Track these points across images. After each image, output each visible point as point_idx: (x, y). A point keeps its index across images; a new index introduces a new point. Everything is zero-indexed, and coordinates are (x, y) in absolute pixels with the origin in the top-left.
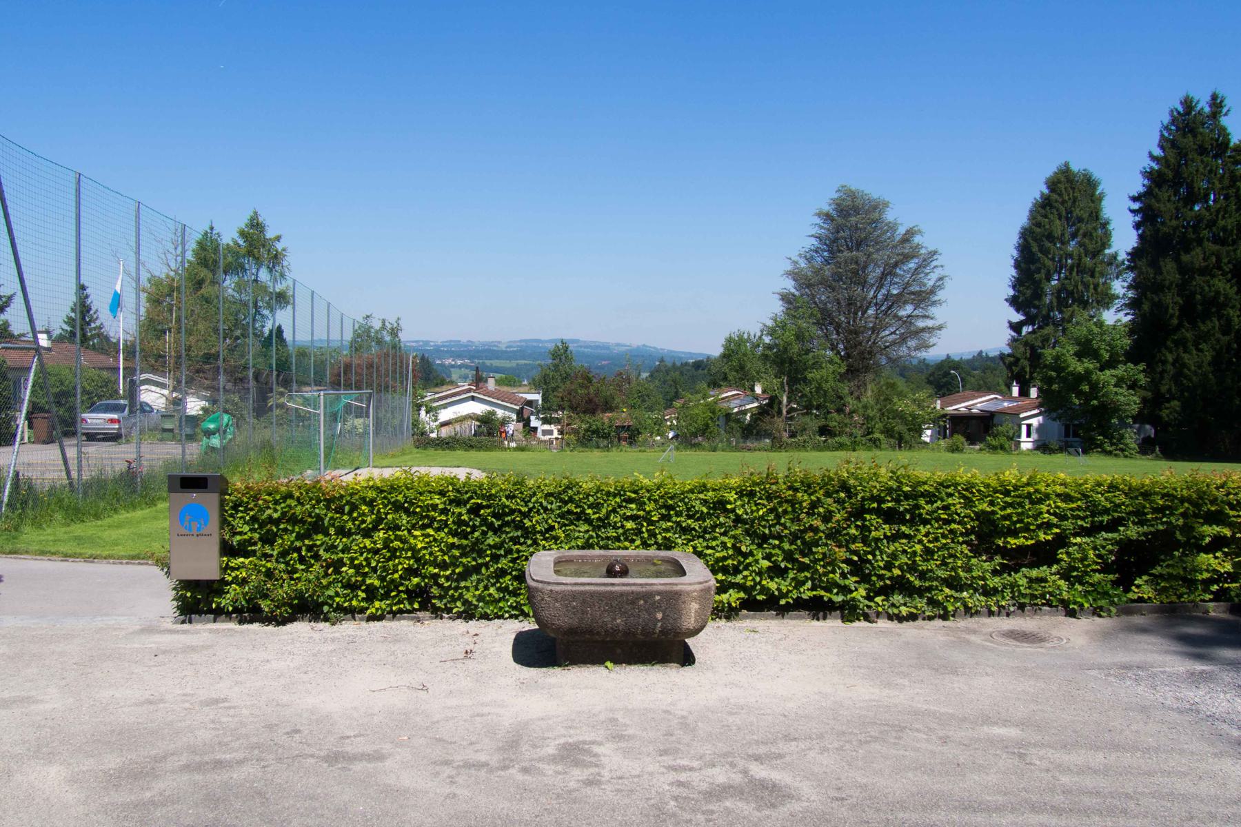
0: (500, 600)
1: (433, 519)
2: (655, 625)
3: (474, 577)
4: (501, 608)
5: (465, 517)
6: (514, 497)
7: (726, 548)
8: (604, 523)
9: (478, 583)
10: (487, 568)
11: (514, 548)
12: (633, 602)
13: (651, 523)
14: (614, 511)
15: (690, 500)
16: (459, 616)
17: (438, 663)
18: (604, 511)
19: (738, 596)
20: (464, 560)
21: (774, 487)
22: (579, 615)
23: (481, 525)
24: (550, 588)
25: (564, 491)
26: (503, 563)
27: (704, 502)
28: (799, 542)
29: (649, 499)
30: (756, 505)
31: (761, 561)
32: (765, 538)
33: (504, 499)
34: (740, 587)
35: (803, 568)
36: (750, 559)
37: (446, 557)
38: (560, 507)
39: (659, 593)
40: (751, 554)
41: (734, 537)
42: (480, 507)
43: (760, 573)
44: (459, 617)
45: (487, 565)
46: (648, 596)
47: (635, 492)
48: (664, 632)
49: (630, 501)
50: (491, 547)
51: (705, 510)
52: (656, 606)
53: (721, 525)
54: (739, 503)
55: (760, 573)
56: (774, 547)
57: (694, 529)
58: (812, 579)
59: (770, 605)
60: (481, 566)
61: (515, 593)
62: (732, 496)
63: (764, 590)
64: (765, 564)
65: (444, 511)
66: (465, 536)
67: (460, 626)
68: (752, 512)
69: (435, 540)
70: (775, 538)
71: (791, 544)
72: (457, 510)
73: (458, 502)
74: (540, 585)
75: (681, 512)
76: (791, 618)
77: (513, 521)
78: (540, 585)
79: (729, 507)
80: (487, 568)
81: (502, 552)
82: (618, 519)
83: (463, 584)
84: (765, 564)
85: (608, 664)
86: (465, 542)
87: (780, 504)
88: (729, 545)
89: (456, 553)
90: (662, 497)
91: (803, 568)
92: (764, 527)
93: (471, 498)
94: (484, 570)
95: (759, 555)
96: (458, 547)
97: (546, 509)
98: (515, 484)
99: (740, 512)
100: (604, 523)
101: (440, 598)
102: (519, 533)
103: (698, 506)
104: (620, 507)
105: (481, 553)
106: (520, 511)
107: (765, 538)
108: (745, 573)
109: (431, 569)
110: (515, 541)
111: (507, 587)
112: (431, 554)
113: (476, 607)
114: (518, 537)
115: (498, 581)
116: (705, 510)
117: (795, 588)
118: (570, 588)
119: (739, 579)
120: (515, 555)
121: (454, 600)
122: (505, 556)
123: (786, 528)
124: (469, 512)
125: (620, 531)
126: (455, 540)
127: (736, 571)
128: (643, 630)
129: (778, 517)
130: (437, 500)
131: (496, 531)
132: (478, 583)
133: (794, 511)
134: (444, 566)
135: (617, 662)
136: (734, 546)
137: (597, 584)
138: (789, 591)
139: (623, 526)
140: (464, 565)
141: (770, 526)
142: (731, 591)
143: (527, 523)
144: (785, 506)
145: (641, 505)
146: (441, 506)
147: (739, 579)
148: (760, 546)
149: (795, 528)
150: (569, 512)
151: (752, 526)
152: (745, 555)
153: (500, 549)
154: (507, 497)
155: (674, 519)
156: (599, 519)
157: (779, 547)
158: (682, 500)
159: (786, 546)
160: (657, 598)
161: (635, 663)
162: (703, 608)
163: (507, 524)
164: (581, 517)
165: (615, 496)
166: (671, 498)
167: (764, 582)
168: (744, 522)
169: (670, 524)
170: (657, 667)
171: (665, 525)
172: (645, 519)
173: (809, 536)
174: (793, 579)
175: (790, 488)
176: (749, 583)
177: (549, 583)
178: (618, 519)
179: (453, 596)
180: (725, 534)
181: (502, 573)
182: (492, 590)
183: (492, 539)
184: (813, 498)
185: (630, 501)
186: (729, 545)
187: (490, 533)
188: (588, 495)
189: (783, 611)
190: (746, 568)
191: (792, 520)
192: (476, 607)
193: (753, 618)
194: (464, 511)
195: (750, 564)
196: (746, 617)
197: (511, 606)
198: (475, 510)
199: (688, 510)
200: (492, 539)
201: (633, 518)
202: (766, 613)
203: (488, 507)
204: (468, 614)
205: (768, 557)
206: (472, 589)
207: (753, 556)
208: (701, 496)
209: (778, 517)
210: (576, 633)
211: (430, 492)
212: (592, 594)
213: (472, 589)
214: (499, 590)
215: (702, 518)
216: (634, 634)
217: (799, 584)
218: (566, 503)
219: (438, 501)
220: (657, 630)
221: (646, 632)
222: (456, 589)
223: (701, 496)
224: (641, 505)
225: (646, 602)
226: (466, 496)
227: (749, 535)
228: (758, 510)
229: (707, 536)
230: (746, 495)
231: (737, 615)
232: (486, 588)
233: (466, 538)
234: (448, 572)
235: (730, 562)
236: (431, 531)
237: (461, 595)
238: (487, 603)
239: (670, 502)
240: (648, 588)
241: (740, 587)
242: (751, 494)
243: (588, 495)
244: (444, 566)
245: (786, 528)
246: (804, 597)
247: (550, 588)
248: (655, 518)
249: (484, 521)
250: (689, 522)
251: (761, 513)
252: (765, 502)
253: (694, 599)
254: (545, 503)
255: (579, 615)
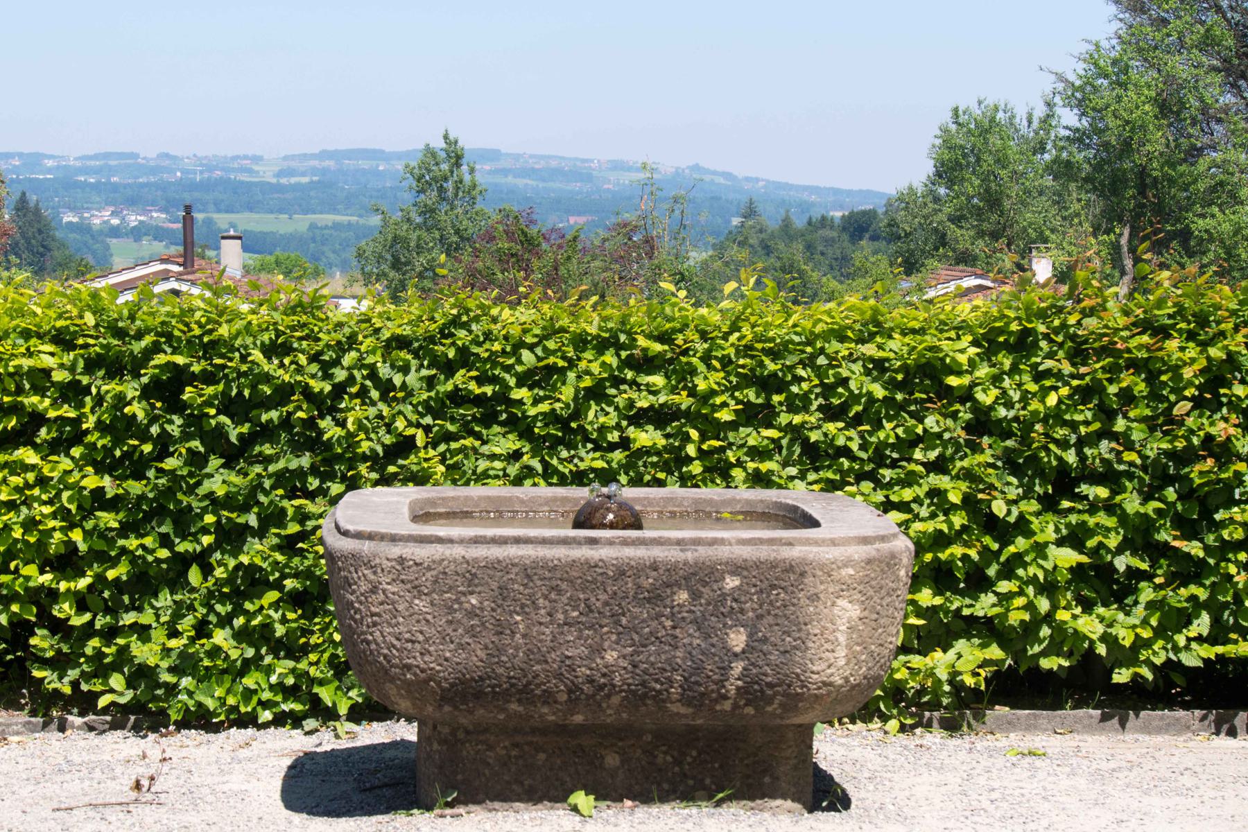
0: (247, 666)
1: (38, 419)
2: (725, 669)
3: (165, 599)
4: (248, 694)
5: (138, 410)
6: (286, 349)
7: (948, 509)
8: (567, 431)
9: (177, 616)
10: (207, 570)
11: (289, 506)
12: (655, 597)
13: (712, 428)
14: (596, 393)
15: (833, 360)
16: (120, 717)
17: (48, 813)
18: (567, 393)
19: (981, 655)
20: (132, 543)
21: (1091, 323)
22: (489, 638)
23: (186, 437)
24: (396, 551)
25: (445, 333)
26: (255, 552)
27: (878, 367)
28: (1171, 493)
29: (706, 358)
30: (1038, 376)
31: (1052, 551)
32: (1064, 483)
33: (257, 355)
34: (989, 629)
35: (1188, 571)
36: (1021, 544)
37: (77, 536)
38: (430, 382)
39: (737, 568)
40: (1023, 526)
41: (968, 475)
42: (180, 377)
43: (1049, 588)
44: (115, 726)
45: (203, 560)
46: (700, 577)
47: (663, 338)
48: (753, 692)
49: (647, 364)
50: (214, 502)
51: (879, 392)
52: (725, 610)
53: (927, 439)
54: (983, 371)
55: (1049, 588)
56: (1093, 508)
57: (846, 452)
58: (1213, 607)
59: (1089, 687)
60: (182, 562)
61: (291, 648)
62: (963, 351)
63: (1063, 640)
64: (1067, 557)
65: (72, 392)
66: (136, 467)
67: (124, 749)
68: (1025, 398)
69: (42, 481)
70: (1096, 479)
71: (1146, 498)
72: (111, 388)
73: (115, 367)
74: (366, 547)
75: (805, 397)
76: (1147, 729)
77: (286, 422)
78: (366, 547)
79: (953, 381)
80: (207, 570)
81: (252, 520)
82: (612, 419)
83: (129, 618)
84: (1067, 557)
85: (580, 798)
86: (135, 487)
87: (1113, 372)
88: (955, 498)
89: (109, 520)
90: (747, 351)
91: (1188, 571)
92: (1064, 444)
93: (156, 349)
94: (194, 576)
95: (1047, 528)
96: (113, 504)
97: (386, 388)
98: (292, 310)
99: (986, 397)
100: (567, 431)
101: (59, 663)
102: (305, 461)
103: (859, 381)
104: (617, 382)
105: (184, 522)
106: (307, 393)
107: (1064, 483)
108: (1004, 586)
109: (30, 570)
110: (292, 483)
111: (267, 627)
112: (30, 524)
113: (172, 690)
114: (300, 473)
115: (238, 610)
116: (879, 392)
117: (1160, 632)
118: (458, 551)
119: (985, 605)
120: (294, 528)
121: (101, 670)
122: (261, 533)
123: (1130, 446)
124: (146, 393)
125: (618, 456)
126: (107, 481)
127: (978, 582)
128: (687, 685)
129: (1107, 414)
130: (47, 357)
131: (233, 456)
132: (177, 616)
133: (1155, 395)
134: (67, 562)
135: (607, 792)
136: (969, 502)
137: (544, 541)
138: (1140, 644)
139: (625, 443)
140: (134, 560)
141: (1081, 443)
142: (961, 645)
143: (330, 429)
144: (1127, 379)
145: (682, 376)
146: (59, 376)
147: (985, 605)
148: (1049, 504)
149: (1157, 446)
150: (458, 397)
151: (1025, 440)
152: (1002, 531)
153: (245, 509)
154: (270, 351)
155: (784, 419)
156: (552, 418)
157: (1110, 508)
158: (809, 362)
159: (1132, 503)
160: (731, 582)
161: (664, 799)
162: (872, 616)
163: (266, 433)
164: (494, 411)
165: (602, 345)
166: (775, 355)
167: (1062, 615)
168: (1001, 430)
169: (773, 433)
170: (733, 810)
171: (753, 437)
172: (690, 417)
173: (1200, 471)
174: (1150, 605)
175: (1146, 325)
176: (1016, 617)
177: (394, 539)
178: (612, 419)
179: (99, 655)
180: (939, 466)
181: (252, 582)
182: (221, 637)
183: (220, 481)
184: (1215, 352)
185: (647, 364)
186: (955, 498)
187: (215, 462)
188: (519, 345)
189: (1123, 703)
190: (1007, 572)
191: (1151, 424)
192: (172, 690)
193: (1030, 728)
194: (131, 389)
195: (1018, 559)
196: (1010, 726)
197: (279, 687)
198: (166, 390)
199: (828, 390)
200: (220, 481)
201: (658, 417)
202: (1068, 713)
203: (208, 378)
204: (145, 715)
205: (1075, 538)
206: (159, 635)
207: (1029, 534)
208: (870, 350)
209: (1107, 414)
210: (479, 695)
211: (26, 334)
212: (528, 571)
213: (159, 635)
214: (242, 636)
215: (871, 415)
216: (659, 699)
217: (1173, 621)
218: (449, 368)
219: (49, 362)
220: (732, 686)
221: (697, 697)
222: (110, 634)
223: (870, 350)
224: (682, 376)
225: (695, 595)
226: (138, 347)
227: (1015, 470)
228: (1045, 392)
229: (887, 474)
230: (1008, 347)
231: (979, 717)
232: (202, 630)
233: (139, 476)
234: (83, 583)
235: (957, 550)
236: (28, 455)
237: (124, 650)
238: (205, 677)
239: (771, 366)
240: (703, 552)
241: (989, 629)
242: (1023, 344)
243: (519, 345)
244: (67, 562)
245: (1130, 446)
246: (1190, 660)
247: (396, 551)
248: (725, 416)
249: (196, 423)
250: (831, 427)
251: (1052, 400)
252: (1067, 368)
253: (845, 588)
254: (384, 371)
255: (489, 638)
